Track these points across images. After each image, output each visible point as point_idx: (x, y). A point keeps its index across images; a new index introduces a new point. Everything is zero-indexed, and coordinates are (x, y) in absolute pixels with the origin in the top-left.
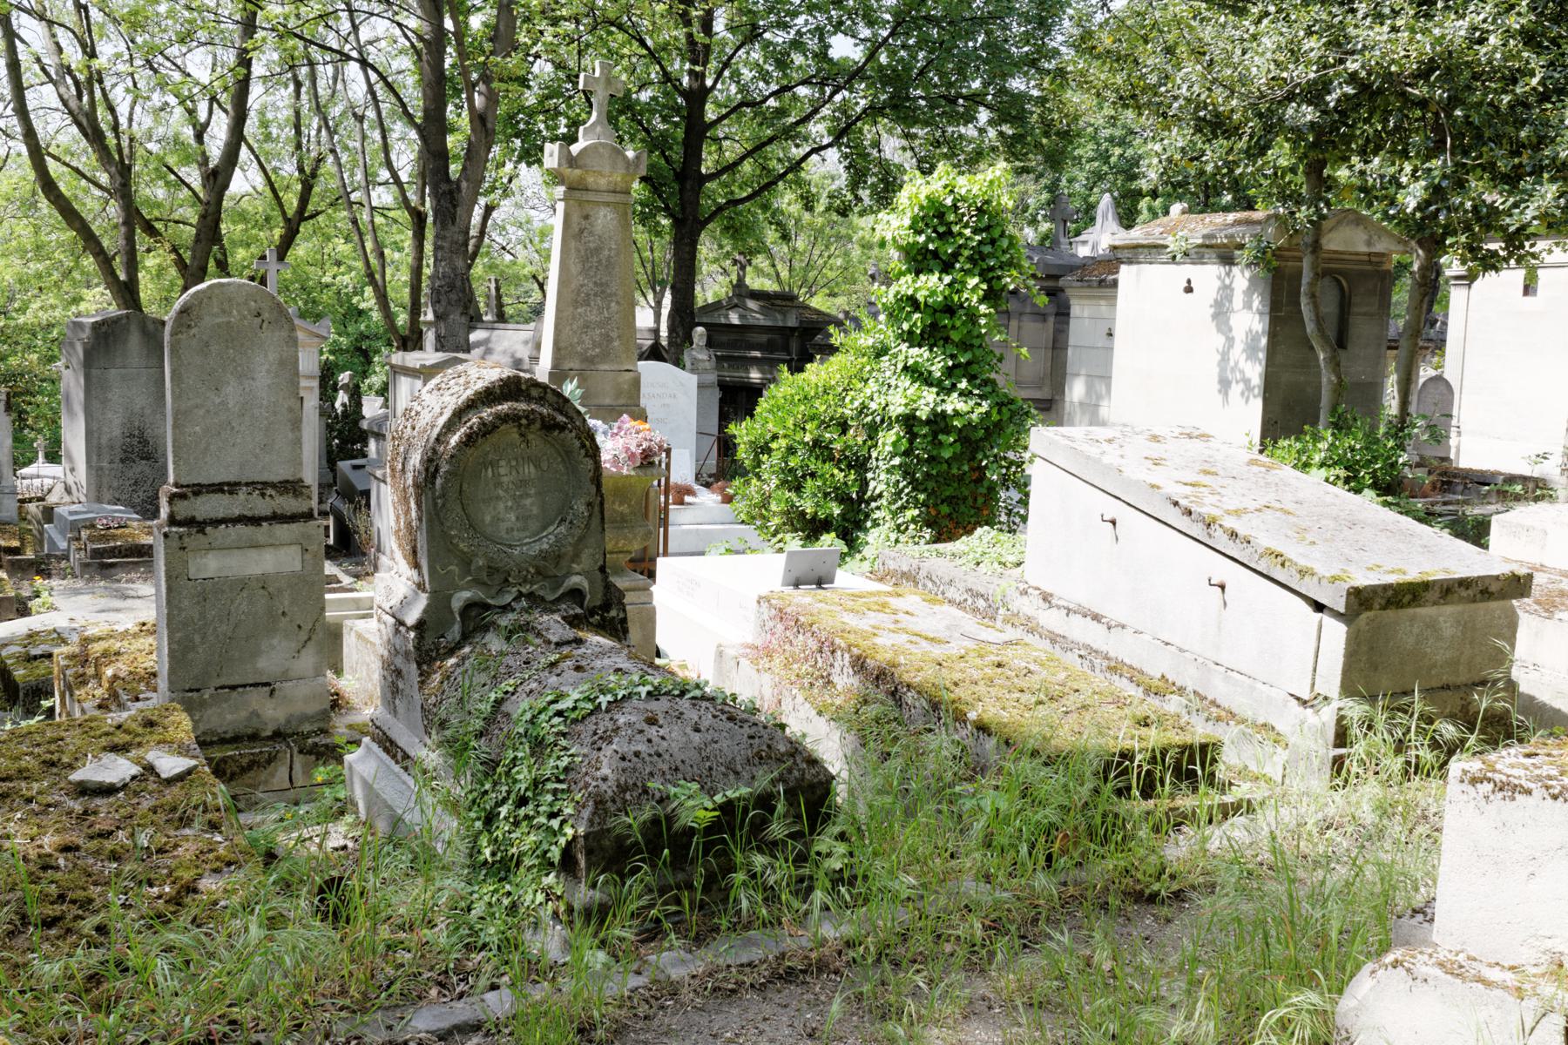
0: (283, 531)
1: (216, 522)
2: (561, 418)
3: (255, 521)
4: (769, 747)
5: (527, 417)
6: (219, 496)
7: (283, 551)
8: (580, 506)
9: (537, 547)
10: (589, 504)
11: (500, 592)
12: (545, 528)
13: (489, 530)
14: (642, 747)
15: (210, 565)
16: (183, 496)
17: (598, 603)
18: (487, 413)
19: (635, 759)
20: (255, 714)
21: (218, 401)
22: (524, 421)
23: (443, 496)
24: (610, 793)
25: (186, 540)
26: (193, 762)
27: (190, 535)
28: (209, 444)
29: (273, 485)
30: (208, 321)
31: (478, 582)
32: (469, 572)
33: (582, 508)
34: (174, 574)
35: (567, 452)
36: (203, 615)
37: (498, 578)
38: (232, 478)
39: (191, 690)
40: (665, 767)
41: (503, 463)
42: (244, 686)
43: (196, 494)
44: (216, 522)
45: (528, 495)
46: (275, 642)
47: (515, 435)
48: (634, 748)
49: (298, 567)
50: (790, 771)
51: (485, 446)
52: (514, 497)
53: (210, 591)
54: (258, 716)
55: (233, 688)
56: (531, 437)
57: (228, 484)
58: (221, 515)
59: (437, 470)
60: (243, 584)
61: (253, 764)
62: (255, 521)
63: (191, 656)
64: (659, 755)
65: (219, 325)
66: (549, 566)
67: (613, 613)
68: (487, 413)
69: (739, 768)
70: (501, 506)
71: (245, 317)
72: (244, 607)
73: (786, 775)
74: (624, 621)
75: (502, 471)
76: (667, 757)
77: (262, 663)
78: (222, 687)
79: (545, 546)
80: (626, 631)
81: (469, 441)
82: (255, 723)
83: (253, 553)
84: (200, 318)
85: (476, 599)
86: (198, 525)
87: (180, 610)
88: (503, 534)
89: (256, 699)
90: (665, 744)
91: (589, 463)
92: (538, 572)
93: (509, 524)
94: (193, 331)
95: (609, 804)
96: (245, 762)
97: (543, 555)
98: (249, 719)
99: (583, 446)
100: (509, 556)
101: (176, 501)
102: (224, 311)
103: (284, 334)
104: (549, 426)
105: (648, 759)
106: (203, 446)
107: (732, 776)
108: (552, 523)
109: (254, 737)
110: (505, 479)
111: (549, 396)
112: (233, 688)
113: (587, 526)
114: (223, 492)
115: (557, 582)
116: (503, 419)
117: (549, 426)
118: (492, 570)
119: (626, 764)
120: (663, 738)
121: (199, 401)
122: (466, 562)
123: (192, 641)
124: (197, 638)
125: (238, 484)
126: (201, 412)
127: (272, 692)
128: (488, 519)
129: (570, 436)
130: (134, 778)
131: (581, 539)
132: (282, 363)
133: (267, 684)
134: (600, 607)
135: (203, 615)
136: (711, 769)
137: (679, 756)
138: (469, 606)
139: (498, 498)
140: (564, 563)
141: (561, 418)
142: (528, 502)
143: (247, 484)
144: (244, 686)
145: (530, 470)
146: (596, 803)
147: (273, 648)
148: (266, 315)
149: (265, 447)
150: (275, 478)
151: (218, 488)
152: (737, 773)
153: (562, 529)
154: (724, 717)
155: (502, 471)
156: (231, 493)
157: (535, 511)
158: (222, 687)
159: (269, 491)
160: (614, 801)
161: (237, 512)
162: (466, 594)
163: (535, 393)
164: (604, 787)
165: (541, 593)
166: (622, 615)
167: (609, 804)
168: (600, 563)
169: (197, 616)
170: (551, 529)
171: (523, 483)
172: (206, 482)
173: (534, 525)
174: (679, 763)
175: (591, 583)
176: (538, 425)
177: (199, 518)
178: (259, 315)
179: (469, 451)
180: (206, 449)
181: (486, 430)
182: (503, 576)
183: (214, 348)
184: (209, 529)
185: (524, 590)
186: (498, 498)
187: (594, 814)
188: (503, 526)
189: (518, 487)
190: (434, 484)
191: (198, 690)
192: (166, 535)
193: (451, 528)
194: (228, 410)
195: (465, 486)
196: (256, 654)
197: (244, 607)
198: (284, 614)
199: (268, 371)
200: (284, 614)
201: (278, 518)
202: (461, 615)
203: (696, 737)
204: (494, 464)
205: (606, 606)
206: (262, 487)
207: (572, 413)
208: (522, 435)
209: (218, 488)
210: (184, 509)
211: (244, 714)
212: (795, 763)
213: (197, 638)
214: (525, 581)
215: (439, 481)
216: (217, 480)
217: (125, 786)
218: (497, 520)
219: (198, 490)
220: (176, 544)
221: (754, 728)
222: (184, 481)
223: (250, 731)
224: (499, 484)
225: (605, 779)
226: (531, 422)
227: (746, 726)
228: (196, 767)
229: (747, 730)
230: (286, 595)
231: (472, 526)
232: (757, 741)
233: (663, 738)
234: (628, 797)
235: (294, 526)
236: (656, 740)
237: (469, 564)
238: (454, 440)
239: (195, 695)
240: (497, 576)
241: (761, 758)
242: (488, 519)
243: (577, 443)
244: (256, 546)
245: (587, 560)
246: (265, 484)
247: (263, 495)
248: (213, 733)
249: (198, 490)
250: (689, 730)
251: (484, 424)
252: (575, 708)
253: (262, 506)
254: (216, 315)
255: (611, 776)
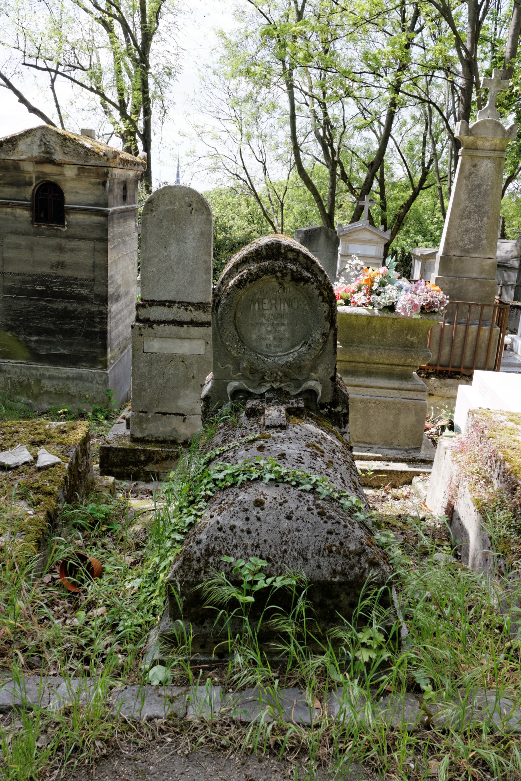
0: (195, 331)
1: (159, 322)
2: (306, 274)
3: (180, 324)
4: (341, 544)
5: (281, 272)
6: (162, 308)
7: (195, 342)
8: (317, 335)
9: (285, 359)
10: (323, 334)
11: (260, 385)
12: (293, 347)
13: (254, 344)
14: (239, 523)
15: (155, 346)
16: (143, 306)
17: (328, 401)
18: (253, 267)
19: (229, 531)
20: (174, 429)
21: (165, 254)
22: (279, 274)
23: (221, 319)
24: (198, 554)
25: (143, 330)
26: (58, 460)
27: (145, 328)
28: (160, 278)
29: (193, 305)
30: (162, 208)
31: (244, 376)
32: (239, 370)
33: (318, 336)
34: (136, 348)
35: (310, 297)
36: (150, 373)
37: (258, 376)
38: (171, 299)
39: (142, 412)
40: (249, 543)
41: (266, 301)
42: (170, 414)
43: (151, 305)
44: (159, 322)
45: (283, 324)
46: (188, 392)
47: (275, 283)
48: (232, 522)
49: (203, 352)
50: (352, 567)
51: (254, 288)
52: (272, 324)
53: (156, 359)
54: (176, 431)
55: (164, 414)
56: (286, 285)
57: (169, 302)
58: (163, 319)
59: (219, 302)
60: (172, 358)
61: (168, 457)
62: (180, 324)
63: (143, 393)
64: (249, 532)
65: (168, 211)
66: (294, 372)
67: (339, 409)
68: (253, 267)
69: (309, 556)
70: (263, 329)
71: (182, 206)
72: (172, 371)
73: (348, 570)
74: (346, 415)
75: (265, 306)
76: (254, 535)
77: (180, 403)
78: (159, 413)
79: (291, 359)
80: (346, 422)
81: (240, 284)
82: (174, 434)
83: (178, 342)
84: (158, 206)
85: (241, 387)
86: (149, 322)
87: (138, 368)
88: (264, 348)
89: (176, 421)
90: (258, 524)
91: (325, 307)
92: (285, 375)
93: (268, 342)
94: (154, 214)
95: (194, 562)
96: (164, 455)
97: (289, 365)
98: (171, 432)
99: (321, 294)
100: (264, 362)
101: (140, 308)
102: (171, 203)
103: (204, 217)
104: (297, 279)
105: (239, 533)
106: (156, 279)
107: (301, 562)
108: (298, 344)
109: (174, 442)
110: (267, 312)
111: (301, 258)
112: (164, 414)
113: (323, 349)
114: (165, 306)
115: (299, 383)
116: (266, 271)
117: (297, 279)
118: (253, 371)
119: (220, 534)
120: (259, 519)
121: (155, 254)
122: (237, 363)
123: (144, 385)
124: (147, 385)
125: (174, 302)
126: (157, 260)
127: (184, 420)
128: (254, 337)
129: (312, 287)
130: (25, 463)
131: (318, 357)
132: (202, 234)
133: (182, 415)
134: (330, 404)
135: (150, 373)
136: (285, 551)
137: (264, 536)
138: (236, 392)
139: (262, 324)
140: (305, 372)
141: (306, 274)
142: (282, 328)
143: (179, 303)
144: (170, 414)
145: (284, 308)
146: (185, 560)
147: (187, 396)
148: (194, 206)
149: (191, 283)
150: (195, 301)
151: (162, 303)
152: (306, 560)
153: (304, 349)
154: (315, 511)
155: (265, 306)
156: (169, 307)
157: (287, 335)
158: (159, 413)
159: (190, 308)
160: (198, 561)
161: (172, 318)
162: (235, 384)
163: (290, 255)
164: (195, 548)
165: (287, 389)
166: (345, 411)
167: (194, 562)
168: (332, 374)
169: (147, 372)
170: (297, 348)
171: (280, 316)
172: (157, 299)
173: (286, 344)
174: (261, 541)
175: (324, 387)
176: (289, 278)
177: (152, 319)
178: (190, 205)
179: (240, 292)
180: (158, 281)
181: (252, 278)
182: (261, 375)
183: (165, 224)
184: (155, 326)
185: (274, 386)
186: (262, 324)
187: (180, 567)
188: (264, 343)
189: (276, 319)
190: (217, 310)
191: (146, 412)
192: (132, 327)
193: (227, 341)
194: (171, 259)
195: (239, 314)
196: (177, 397)
197: (172, 371)
198: (193, 377)
199: (194, 239)
200: (193, 377)
201: (194, 323)
202: (231, 396)
203: (285, 524)
204: (260, 302)
205: (334, 404)
206: (186, 305)
207: (316, 271)
208: (280, 284)
209: (162, 303)
210: (145, 313)
211: (169, 429)
212: (359, 561)
213: (147, 385)
214: (276, 380)
215: (220, 309)
216: (163, 299)
217: (17, 467)
218: (260, 338)
219: (151, 303)
220: (137, 332)
221: (336, 526)
222: (146, 298)
223: (172, 439)
224: (262, 315)
225: (199, 542)
226: (284, 276)
227: (330, 522)
228: (59, 463)
229: (329, 526)
230: (195, 367)
231: (242, 341)
232: (333, 536)
233: (259, 519)
234: (211, 560)
235: (201, 329)
236: (253, 519)
237: (239, 364)
238: (231, 283)
239: (144, 415)
240: (256, 374)
241: (331, 551)
242: (254, 337)
243: (317, 292)
244: (180, 338)
245: (321, 371)
246: (189, 303)
247: (186, 309)
248: (152, 436)
249: (151, 303)
250: (282, 517)
251: (251, 274)
252: (222, 480)
253: (185, 316)
254: (167, 205)
255: (204, 541)
